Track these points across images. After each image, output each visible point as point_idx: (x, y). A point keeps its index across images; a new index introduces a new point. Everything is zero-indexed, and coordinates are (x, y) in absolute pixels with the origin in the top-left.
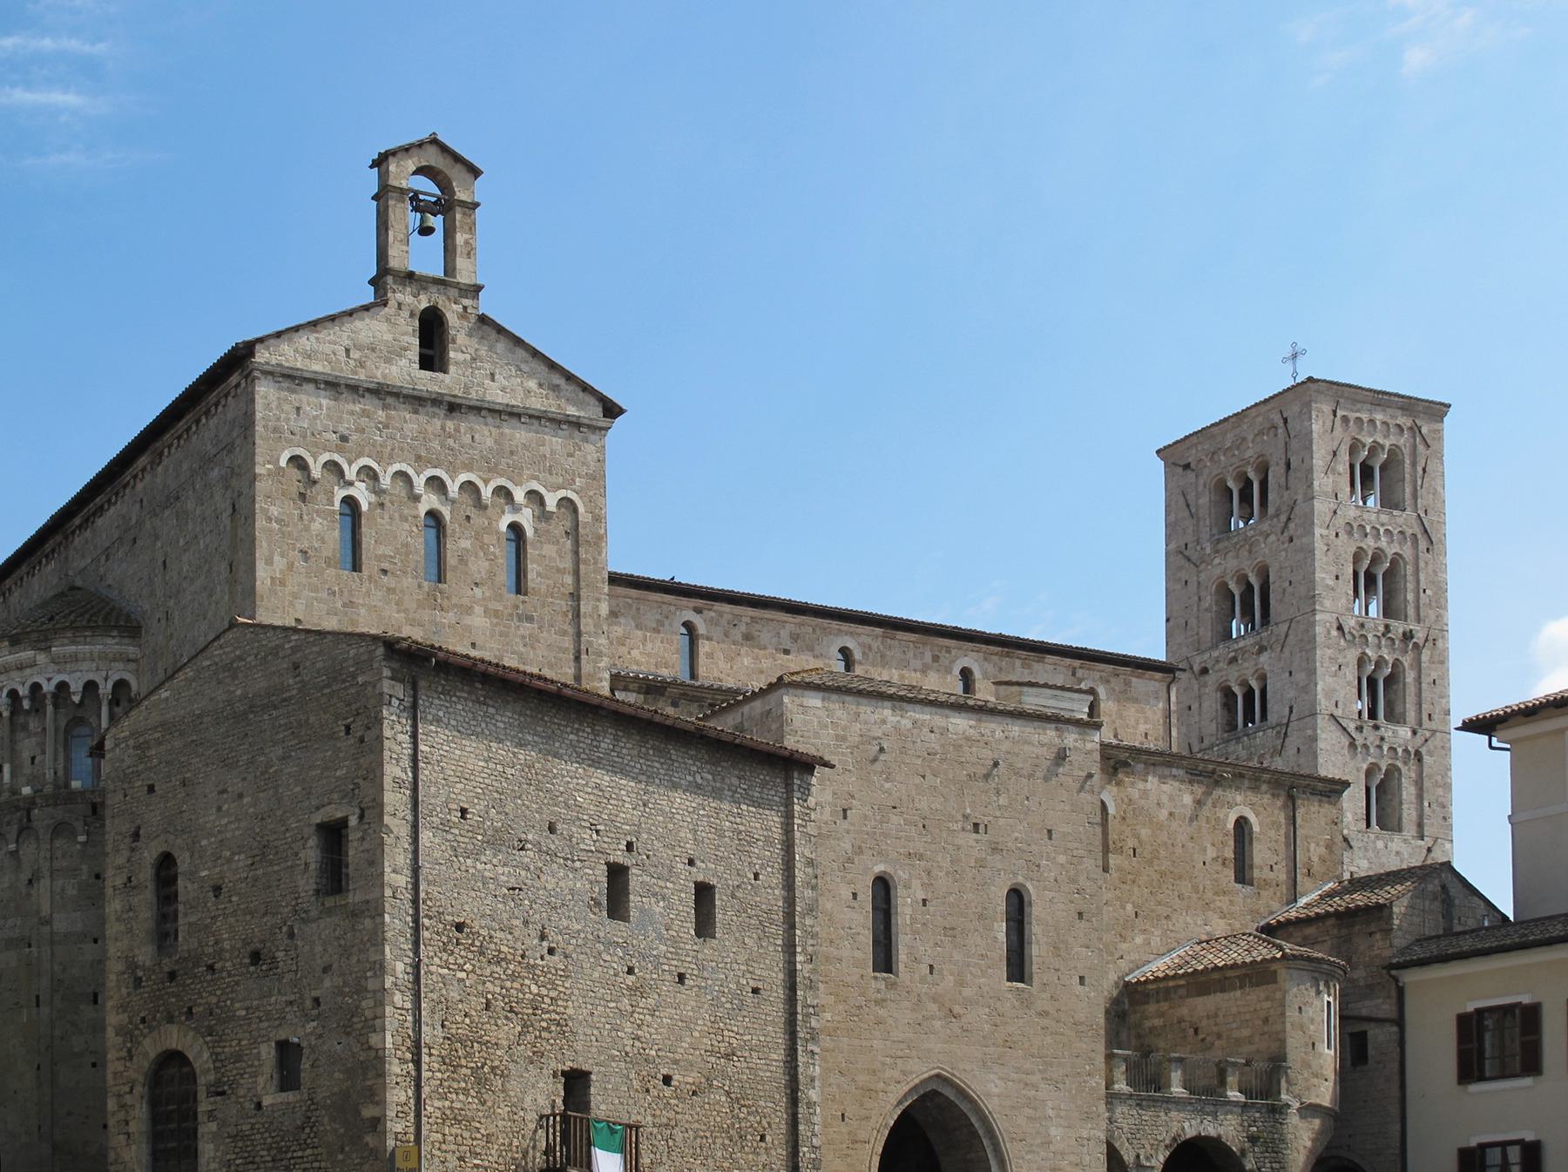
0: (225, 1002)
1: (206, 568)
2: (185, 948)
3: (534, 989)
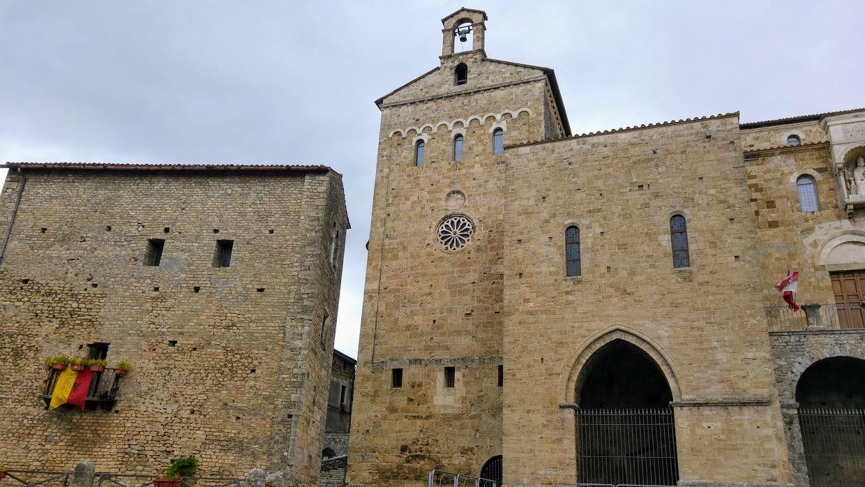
3: (75, 305)
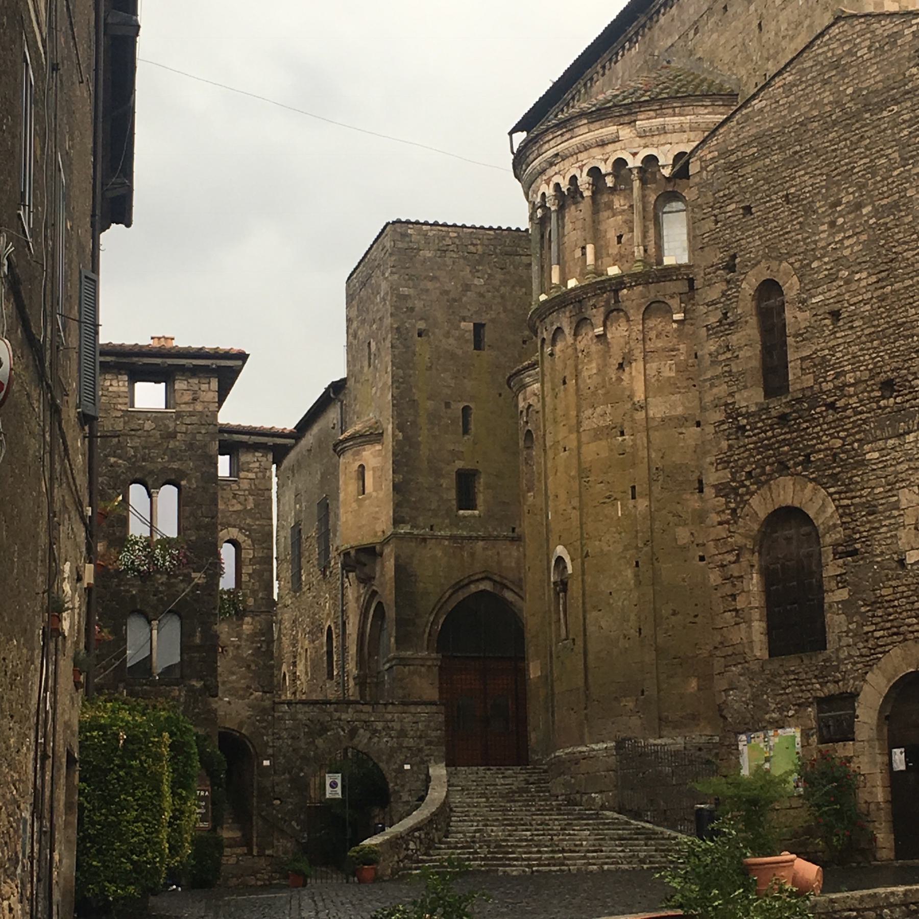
0: (851, 444)
1: (807, 23)
2: (798, 386)
